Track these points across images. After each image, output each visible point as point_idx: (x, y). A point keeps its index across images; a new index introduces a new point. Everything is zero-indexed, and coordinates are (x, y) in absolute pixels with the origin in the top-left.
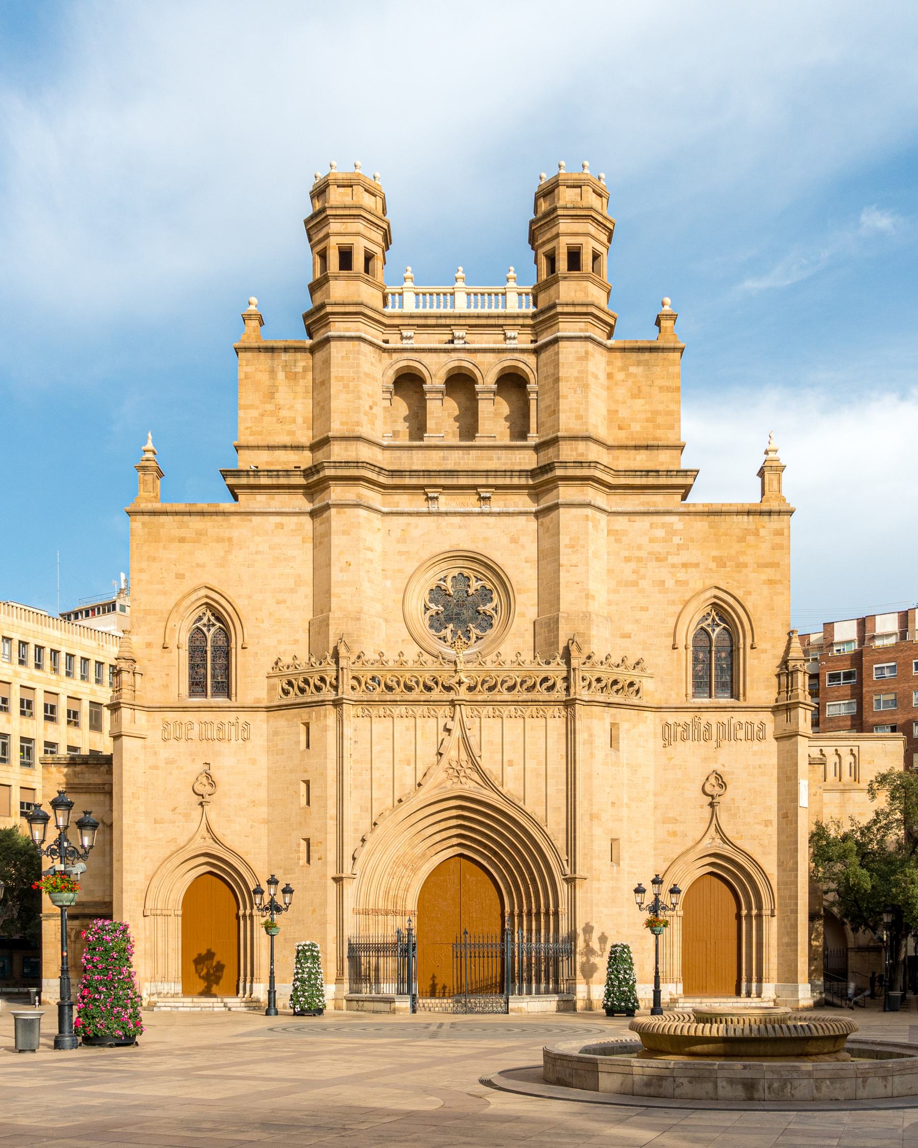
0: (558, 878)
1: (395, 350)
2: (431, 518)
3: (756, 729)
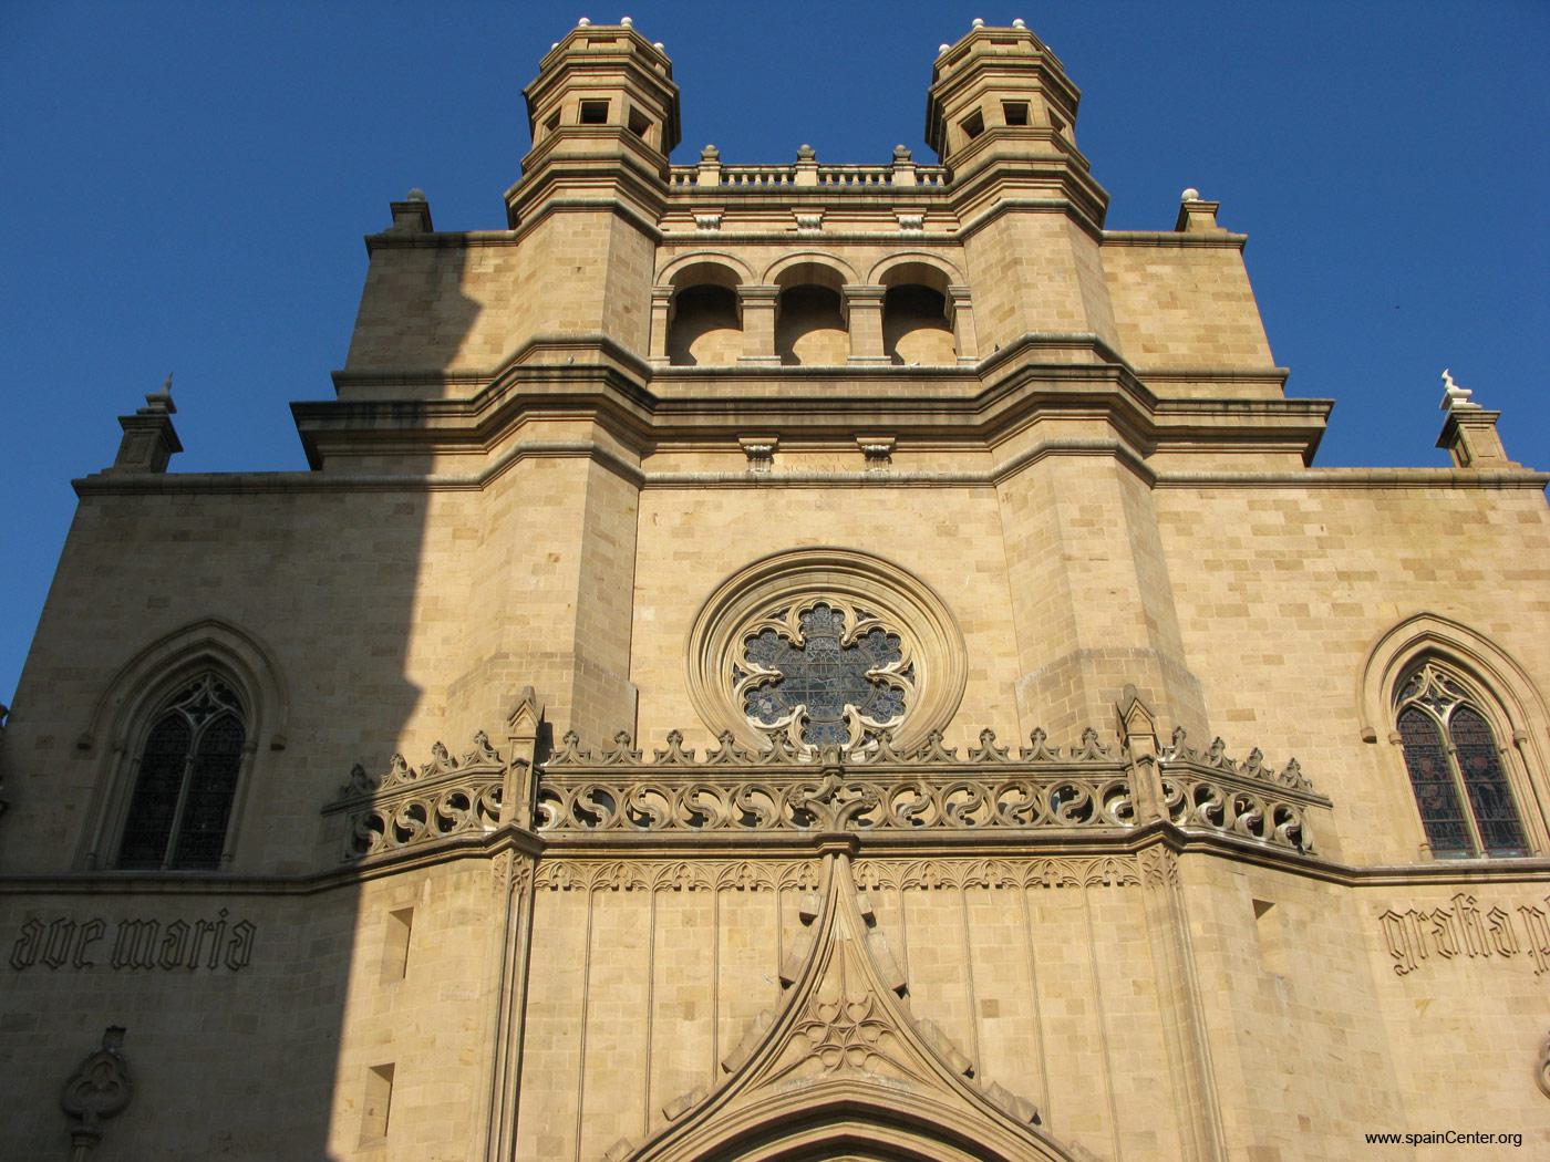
2: (752, 493)
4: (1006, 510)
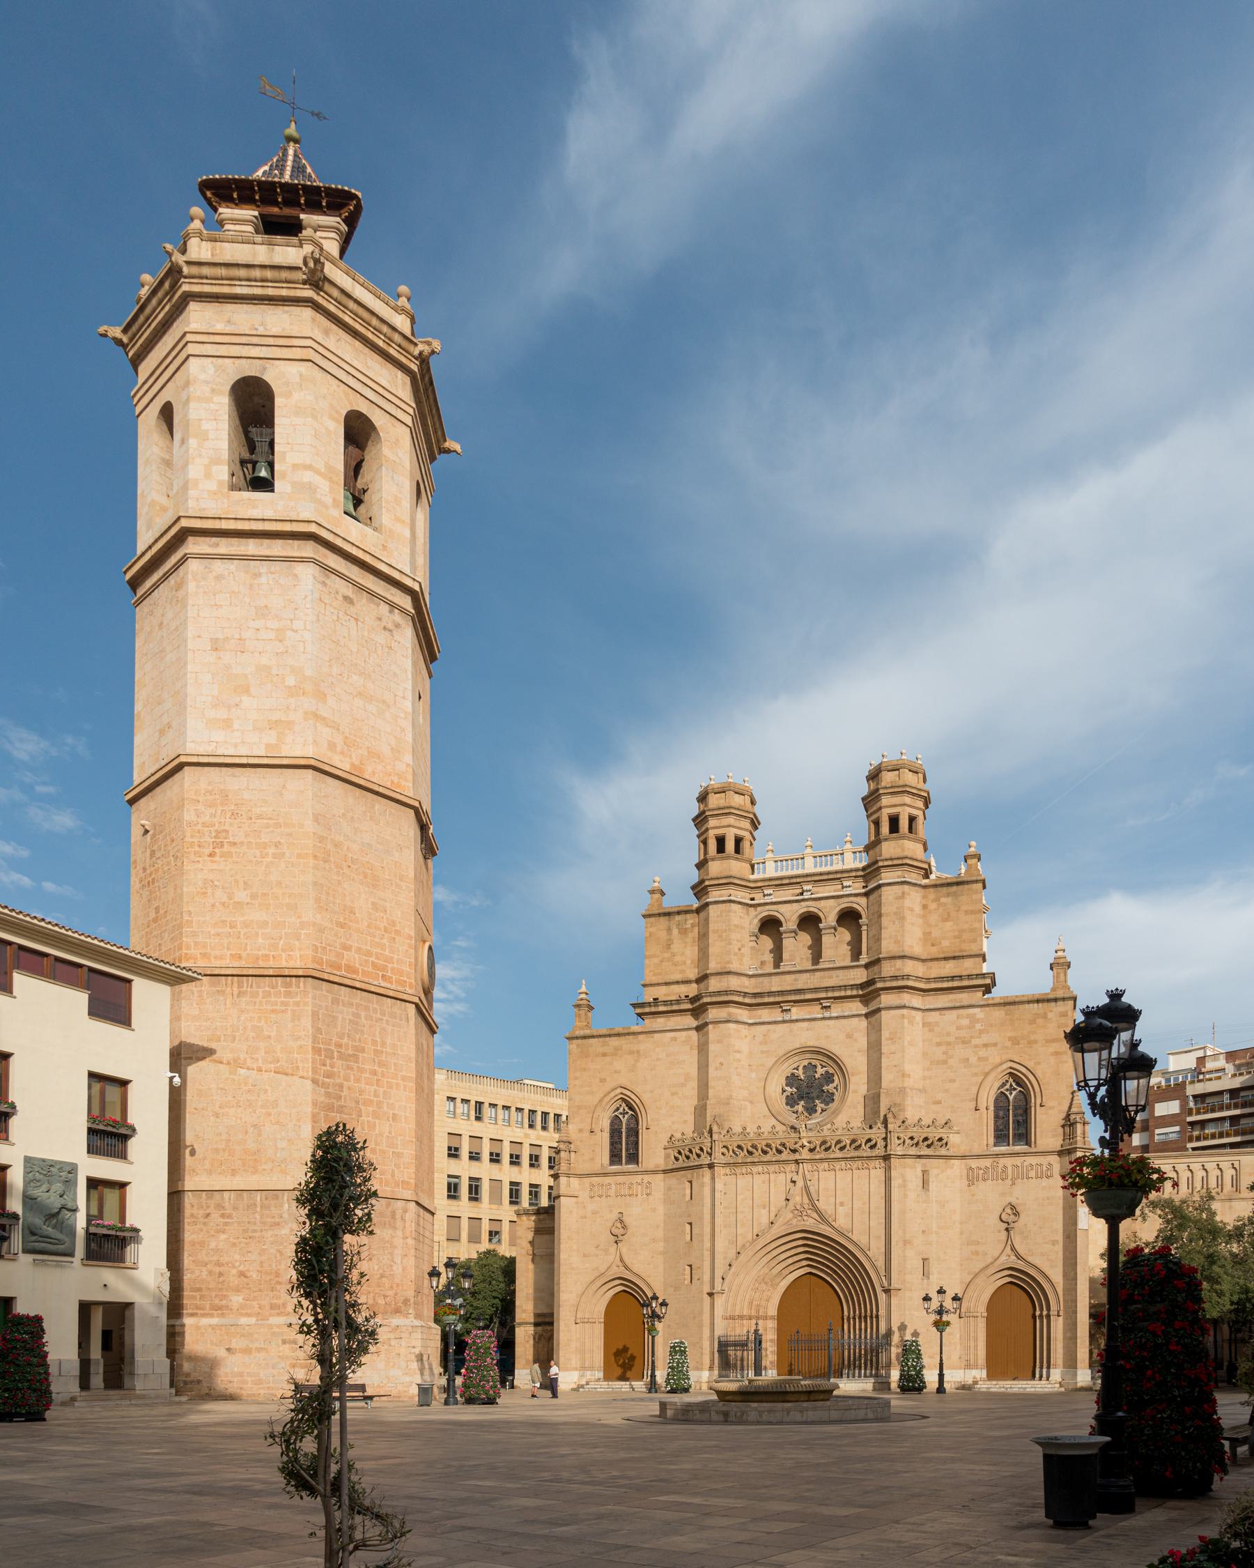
0: (878, 1289)
1: (759, 905)
3: (1045, 1168)
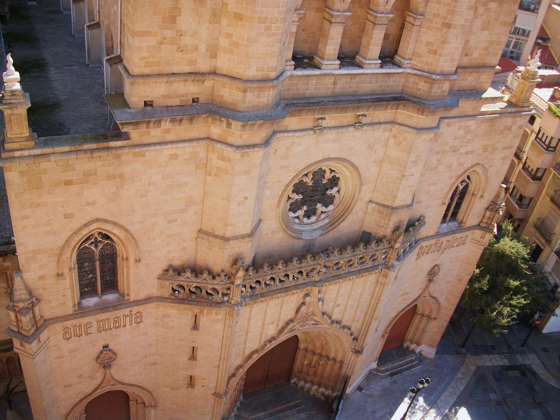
4: (392, 141)
